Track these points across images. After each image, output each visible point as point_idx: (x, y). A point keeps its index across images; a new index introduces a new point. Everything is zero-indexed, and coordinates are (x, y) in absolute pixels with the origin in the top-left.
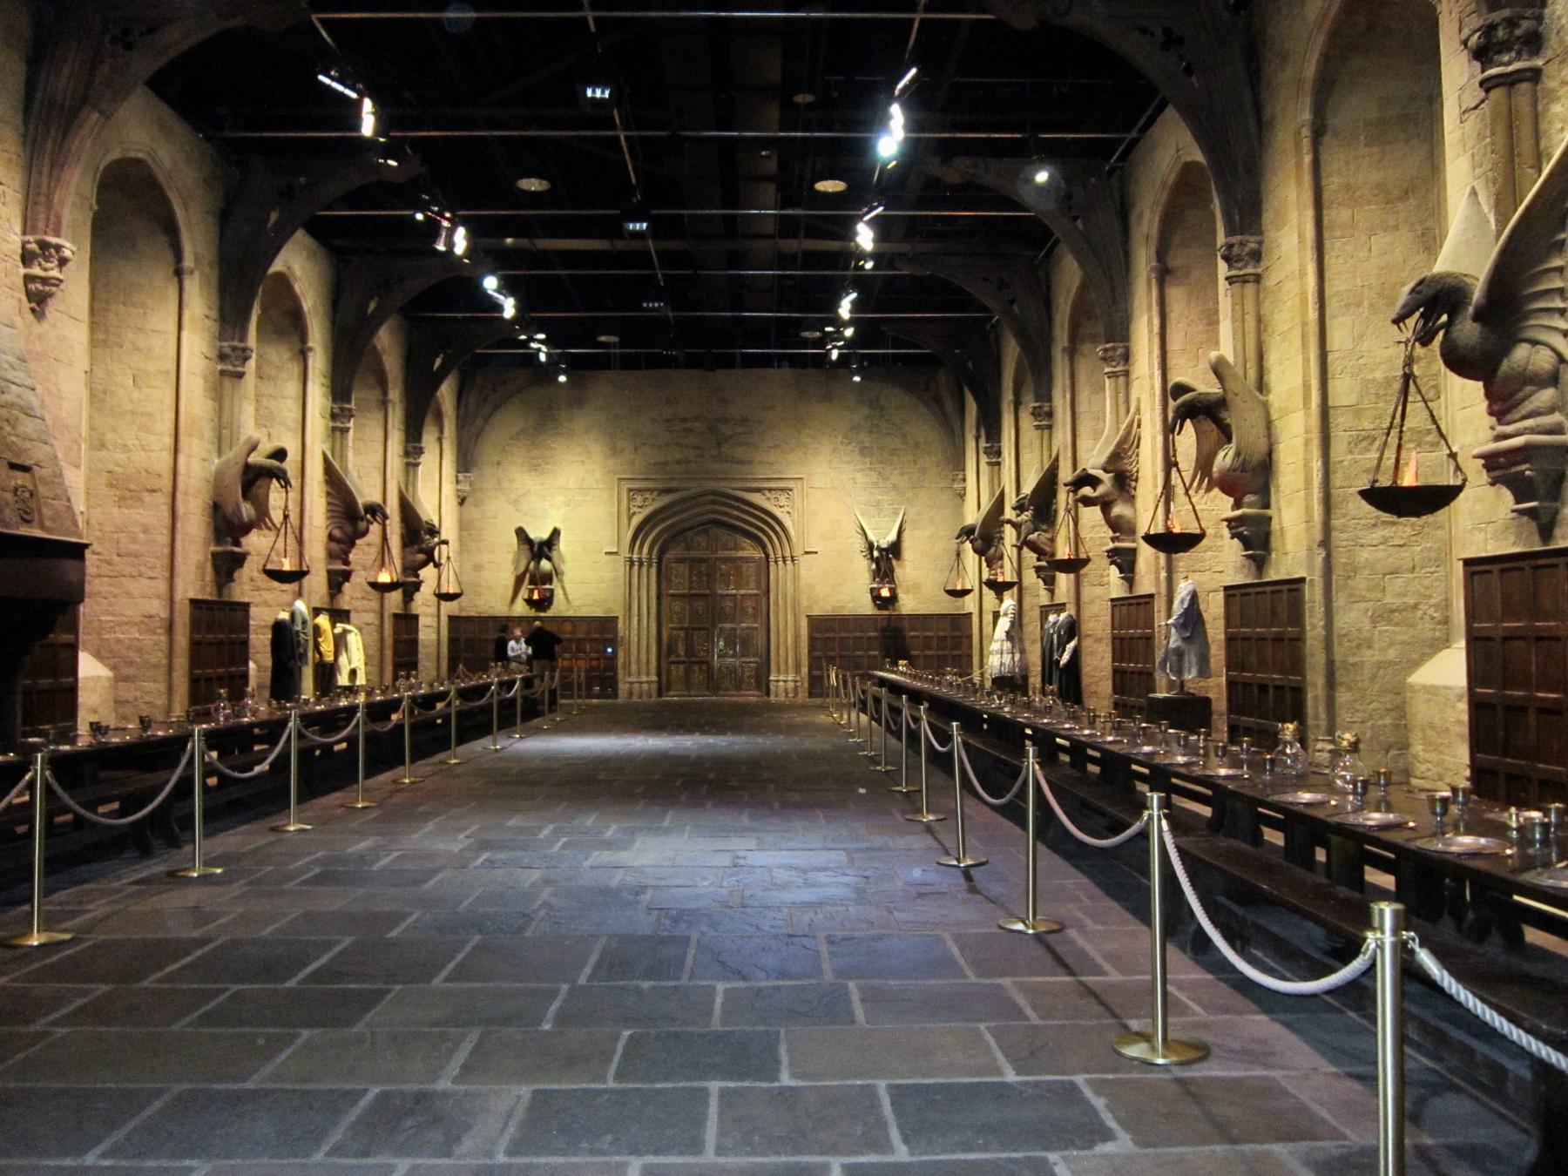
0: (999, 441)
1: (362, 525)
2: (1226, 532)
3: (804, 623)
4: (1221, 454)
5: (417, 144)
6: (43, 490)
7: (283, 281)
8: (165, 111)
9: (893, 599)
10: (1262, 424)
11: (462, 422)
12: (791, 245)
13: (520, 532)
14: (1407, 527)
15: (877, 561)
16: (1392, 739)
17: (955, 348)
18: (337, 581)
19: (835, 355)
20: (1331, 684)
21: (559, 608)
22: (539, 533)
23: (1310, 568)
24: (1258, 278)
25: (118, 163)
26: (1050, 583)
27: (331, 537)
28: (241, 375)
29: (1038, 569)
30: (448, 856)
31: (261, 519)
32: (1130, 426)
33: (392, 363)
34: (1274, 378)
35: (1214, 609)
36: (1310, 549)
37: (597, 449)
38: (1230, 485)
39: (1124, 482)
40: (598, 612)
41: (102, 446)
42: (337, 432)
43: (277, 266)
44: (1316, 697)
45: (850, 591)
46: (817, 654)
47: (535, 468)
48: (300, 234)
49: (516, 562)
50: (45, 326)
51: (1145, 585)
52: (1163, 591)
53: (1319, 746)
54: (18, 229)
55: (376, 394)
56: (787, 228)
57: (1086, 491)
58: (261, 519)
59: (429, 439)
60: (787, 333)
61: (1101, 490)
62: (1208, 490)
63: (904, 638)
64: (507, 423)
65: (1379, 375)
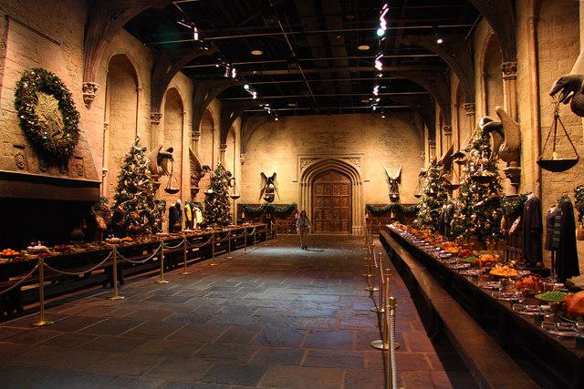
1: (203, 173)
5: (216, 41)
6: (86, 165)
7: (175, 90)
8: (133, 38)
9: (398, 198)
11: (242, 136)
12: (354, 69)
13: (262, 174)
14: (560, 176)
17: (417, 108)
18: (194, 192)
19: (374, 108)
21: (276, 201)
22: (269, 175)
24: (515, 78)
25: (117, 56)
27: (192, 177)
28: (158, 123)
30: (204, 292)
31: (164, 172)
33: (216, 117)
34: (522, 117)
36: (533, 182)
37: (290, 144)
38: (505, 157)
40: (290, 203)
41: (113, 149)
42: (194, 141)
43: (172, 85)
45: (381, 196)
47: (268, 151)
48: (179, 74)
49: (261, 185)
50: (90, 111)
54: (81, 80)
55: (210, 127)
56: (352, 63)
58: (164, 172)
59: (229, 142)
60: (357, 101)
64: (258, 135)
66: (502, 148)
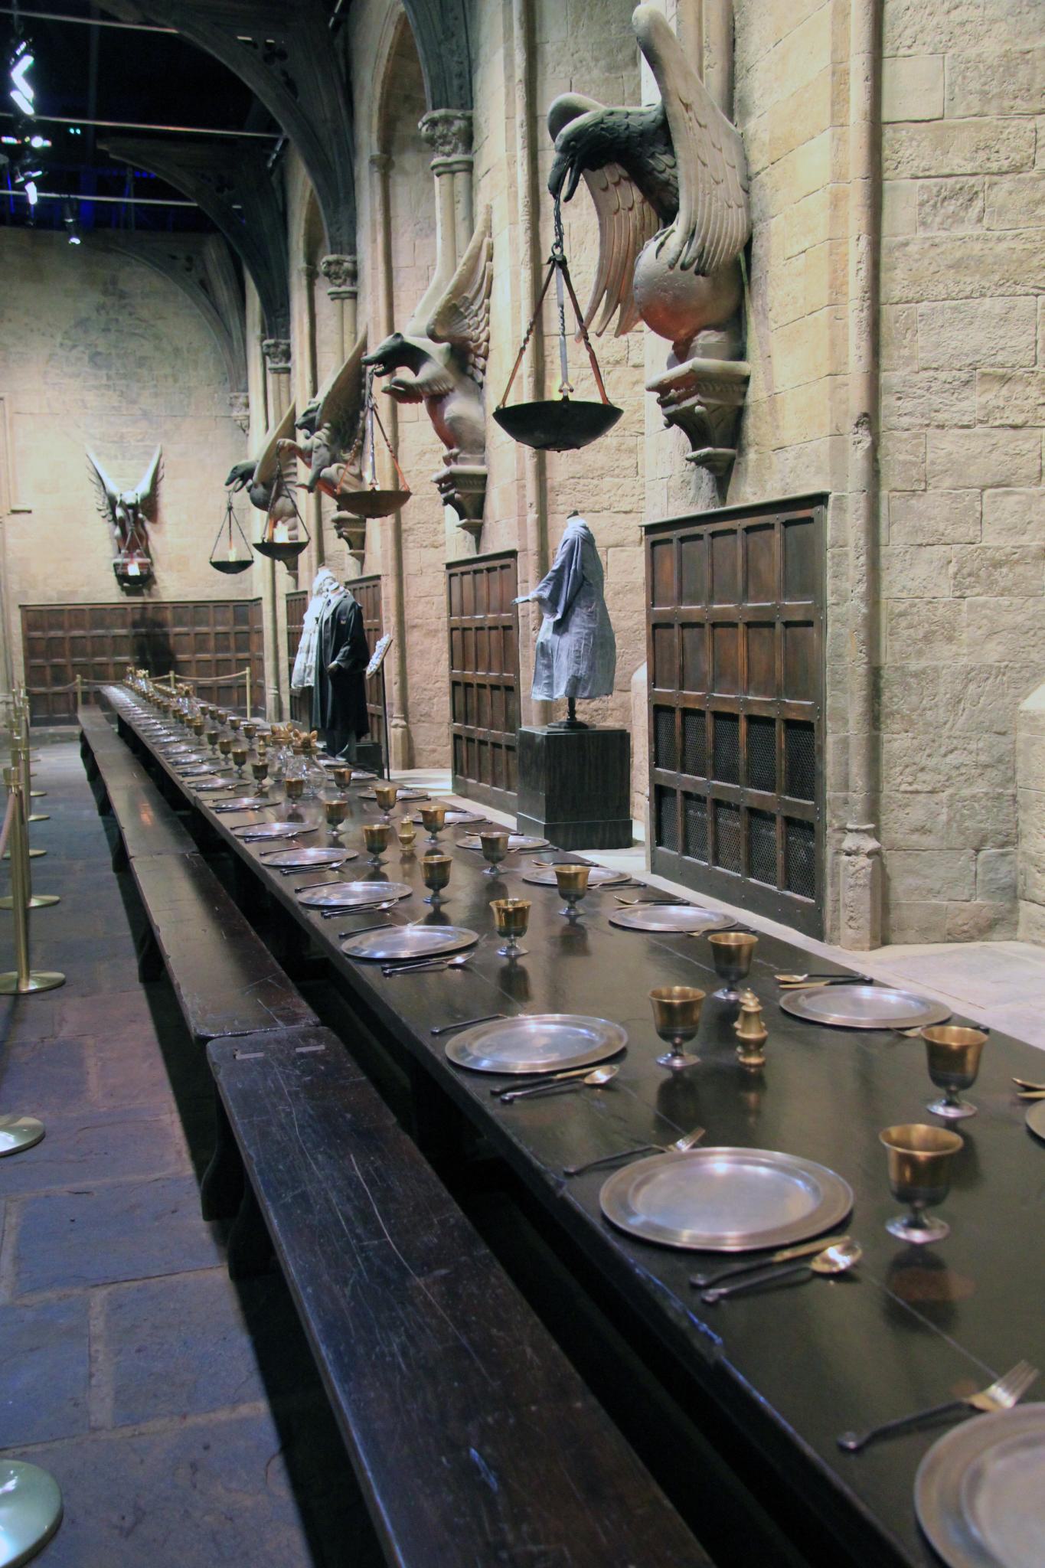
0: (287, 335)
2: (655, 414)
3: (16, 619)
4: (652, 246)
9: (144, 582)
10: (734, 179)
15: (121, 523)
16: (988, 826)
20: (874, 718)
23: (838, 471)
26: (357, 543)
29: (339, 523)
32: (475, 258)
35: (625, 573)
36: (837, 434)
38: (666, 313)
39: (465, 358)
44: (844, 743)
46: (38, 661)
51: (500, 536)
52: (533, 545)
53: (850, 842)
57: (404, 374)
61: (427, 372)
62: (623, 329)
63: (166, 635)
65: (991, 48)
66: (650, 260)
